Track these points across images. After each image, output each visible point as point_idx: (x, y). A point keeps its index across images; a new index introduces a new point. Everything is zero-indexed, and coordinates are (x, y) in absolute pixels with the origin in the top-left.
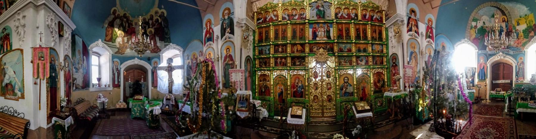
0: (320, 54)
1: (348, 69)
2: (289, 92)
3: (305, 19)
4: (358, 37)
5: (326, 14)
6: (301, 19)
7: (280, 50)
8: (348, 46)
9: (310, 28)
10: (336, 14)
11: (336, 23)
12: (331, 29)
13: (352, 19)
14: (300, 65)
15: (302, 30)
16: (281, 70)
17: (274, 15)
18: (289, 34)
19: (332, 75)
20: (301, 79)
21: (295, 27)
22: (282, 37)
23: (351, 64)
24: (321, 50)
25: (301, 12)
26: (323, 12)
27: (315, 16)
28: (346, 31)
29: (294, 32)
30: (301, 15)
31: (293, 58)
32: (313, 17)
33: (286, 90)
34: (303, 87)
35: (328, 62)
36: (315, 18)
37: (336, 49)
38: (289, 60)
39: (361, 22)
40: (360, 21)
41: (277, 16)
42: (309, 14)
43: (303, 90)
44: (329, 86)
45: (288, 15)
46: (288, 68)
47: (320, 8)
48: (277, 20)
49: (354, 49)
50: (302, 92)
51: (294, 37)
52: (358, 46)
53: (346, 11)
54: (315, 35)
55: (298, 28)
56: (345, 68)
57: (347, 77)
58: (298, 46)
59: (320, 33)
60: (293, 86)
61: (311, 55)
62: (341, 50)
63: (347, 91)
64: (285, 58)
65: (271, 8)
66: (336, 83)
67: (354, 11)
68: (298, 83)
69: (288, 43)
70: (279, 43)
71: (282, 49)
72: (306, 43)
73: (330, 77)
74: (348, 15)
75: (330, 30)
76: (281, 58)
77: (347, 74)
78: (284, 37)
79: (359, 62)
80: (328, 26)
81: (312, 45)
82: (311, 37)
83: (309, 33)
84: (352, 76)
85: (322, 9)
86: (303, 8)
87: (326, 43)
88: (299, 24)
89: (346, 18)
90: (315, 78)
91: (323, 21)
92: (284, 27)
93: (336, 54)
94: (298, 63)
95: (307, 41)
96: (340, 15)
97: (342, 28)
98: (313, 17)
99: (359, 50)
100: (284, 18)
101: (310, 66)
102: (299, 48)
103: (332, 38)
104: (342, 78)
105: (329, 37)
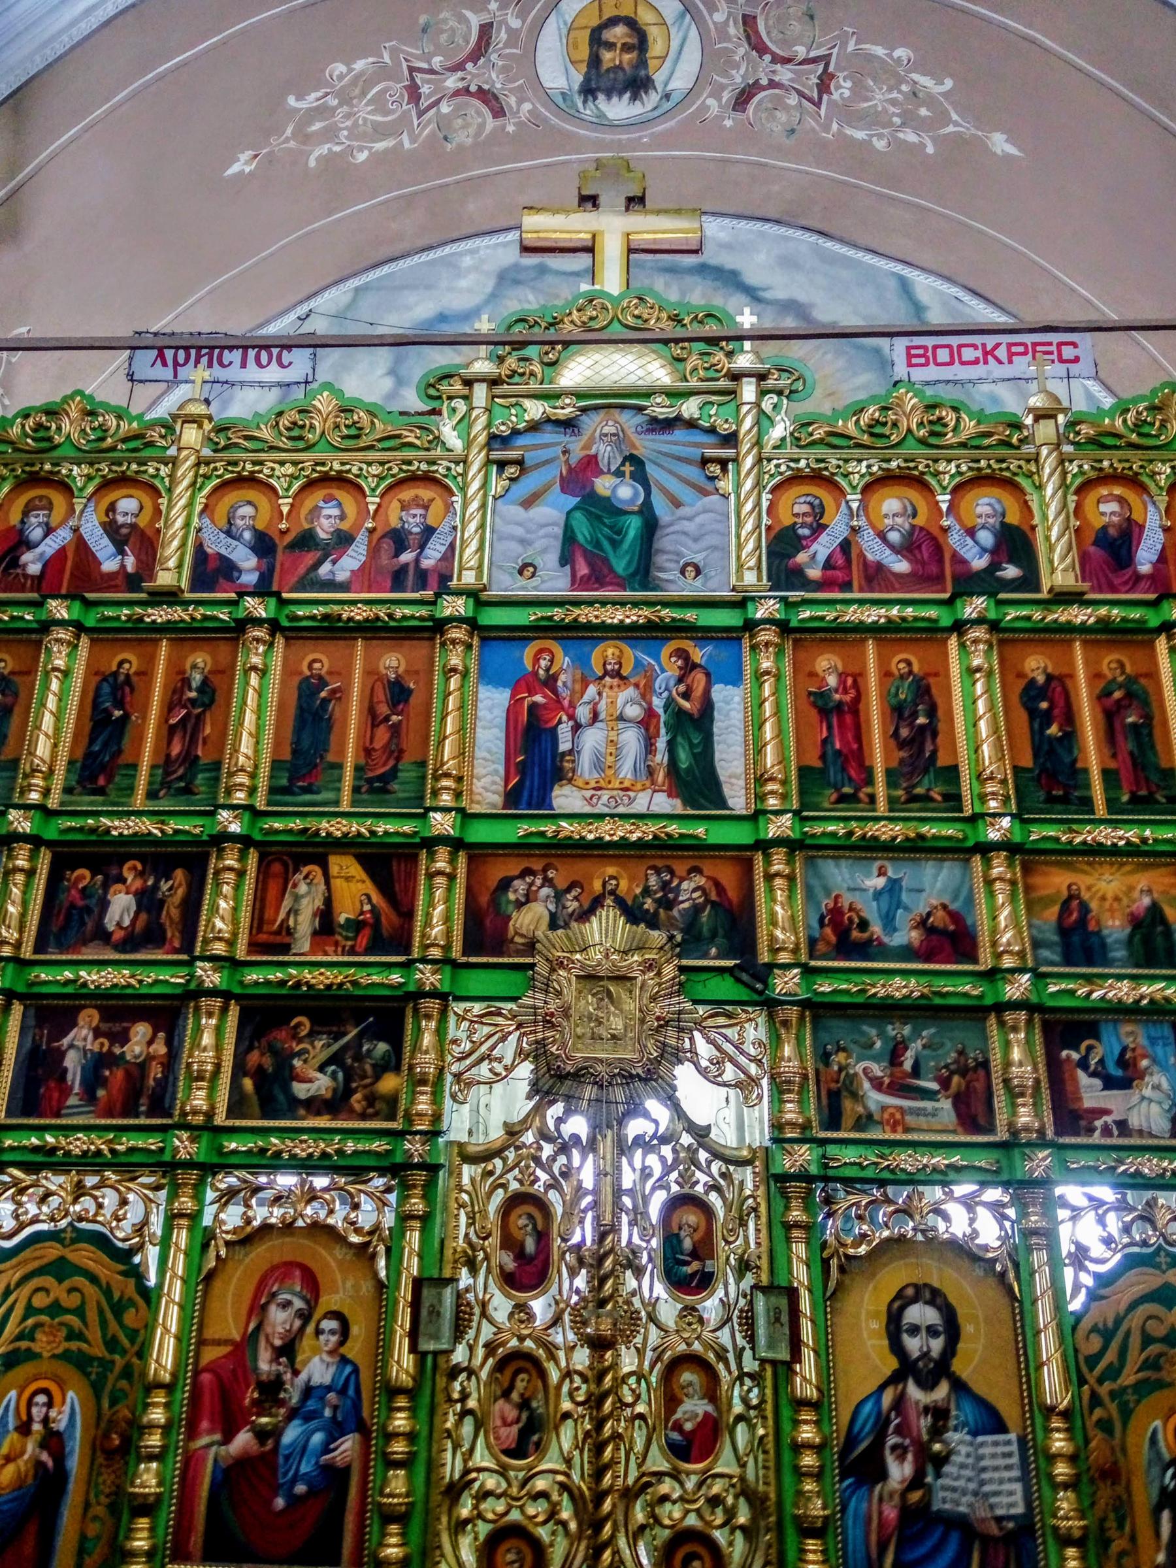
0: (590, 978)
1: (944, 1177)
2: (148, 1479)
3: (441, 581)
4: (1049, 779)
5: (664, 542)
6: (398, 579)
7: (121, 907)
8: (932, 886)
9: (487, 676)
10: (783, 546)
11: (784, 628)
12: (719, 692)
13: (969, 583)
14: (334, 1105)
15: (399, 693)
16: (91, 1162)
17: (111, 529)
18: (252, 733)
19: (725, 1254)
20: (343, 1291)
21: (319, 659)
22: (165, 764)
23: (974, 1112)
24: (605, 932)
25: (393, 517)
26: (633, 526)
27: (549, 560)
28: (898, 712)
29: (310, 714)
30: (399, 539)
31: (263, 1017)
32: (526, 568)
33: (117, 1445)
34: (350, 1409)
35: (685, 1077)
36: (554, 581)
37: (781, 918)
38: (211, 1039)
39: (1078, 615)
40: (1063, 598)
41: (142, 541)
42: (500, 540)
43: (348, 1446)
44: (694, 1408)
45: (263, 545)
46: (183, 1145)
47: (603, 485)
48: (132, 582)
49: (1003, 924)
50: (333, 1478)
51: (303, 761)
52: (1058, 881)
53: (890, 504)
54: (537, 760)
55: (358, 670)
56: (906, 1161)
57: (935, 1298)
58: (344, 866)
59: (592, 739)
60: (225, 1389)
61: (476, 982)
62: (844, 936)
63: (942, 1502)
64: (168, 1013)
65: (90, 457)
66: (784, 1370)
67: (984, 505)
68: (287, 1350)
69: (221, 839)
70: (121, 827)
71: (148, 901)
72: (430, 843)
73: (705, 1282)
74: (924, 546)
75: (708, 706)
76: (118, 1010)
77: (935, 1245)
78: (190, 770)
79: (1089, 1092)
80: (689, 666)
81: (497, 871)
82: (488, 784)
83: (475, 729)
84: (1007, 1278)
85: (626, 492)
86: (428, 479)
87: (661, 847)
88: (372, 630)
89: (902, 581)
90: (510, 1281)
91: (630, 616)
92: (200, 661)
93: (786, 983)
94: (321, 1084)
95: (442, 823)
96: (824, 547)
97: (854, 680)
98: (526, 568)
99: (1077, 940)
100: (210, 571)
101: (458, 1123)
102: (353, 890)
103: (738, 799)
104: (867, 1304)
105: (698, 785)
